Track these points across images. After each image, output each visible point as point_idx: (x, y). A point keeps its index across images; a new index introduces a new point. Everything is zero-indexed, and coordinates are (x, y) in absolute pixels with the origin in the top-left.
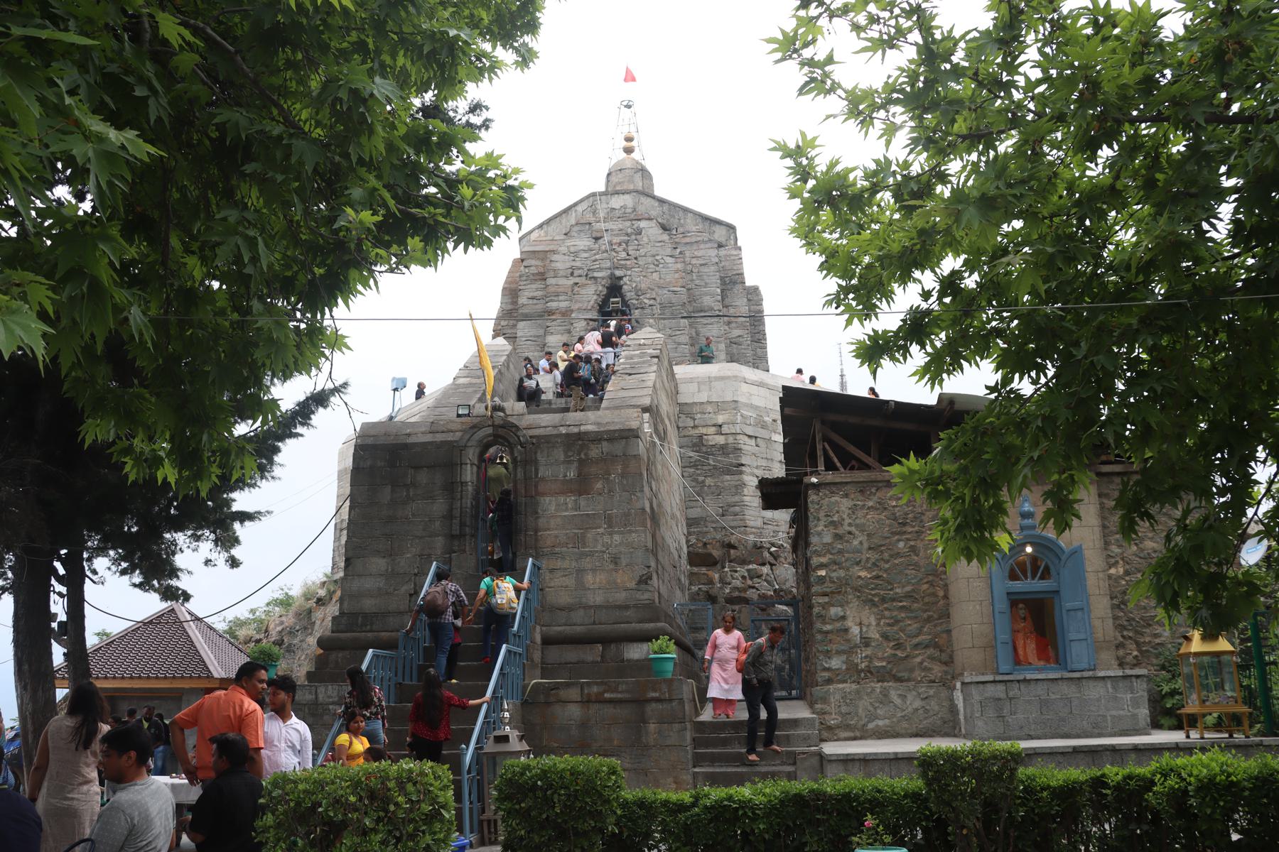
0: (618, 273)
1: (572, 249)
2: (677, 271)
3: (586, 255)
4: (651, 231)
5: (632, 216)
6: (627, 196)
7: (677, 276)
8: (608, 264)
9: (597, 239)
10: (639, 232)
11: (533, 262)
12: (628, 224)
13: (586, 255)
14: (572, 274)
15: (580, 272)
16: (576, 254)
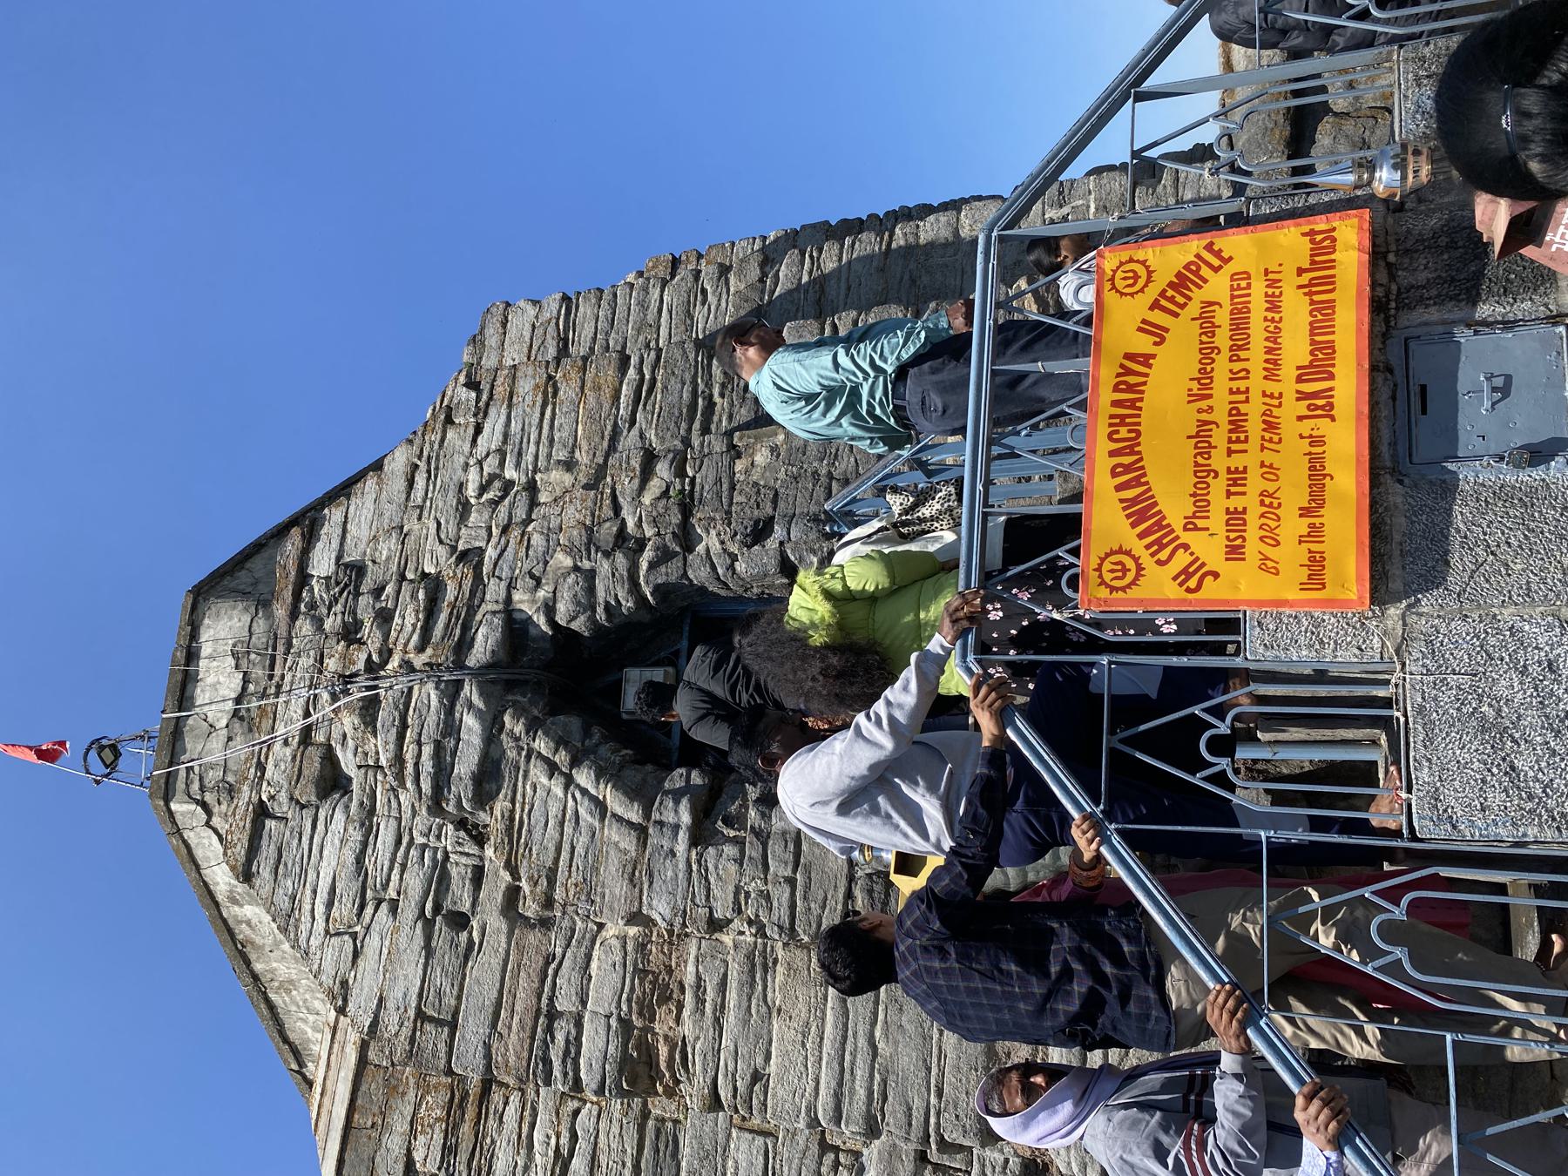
0: (485, 642)
1: (344, 909)
2: (549, 391)
3: (386, 836)
4: (360, 531)
5: (280, 612)
6: (205, 635)
7: (567, 392)
8: (428, 695)
9: (332, 782)
10: (352, 573)
11: (394, 1143)
12: (304, 627)
13: (386, 836)
14: (459, 921)
15: (459, 871)
16: (369, 895)
